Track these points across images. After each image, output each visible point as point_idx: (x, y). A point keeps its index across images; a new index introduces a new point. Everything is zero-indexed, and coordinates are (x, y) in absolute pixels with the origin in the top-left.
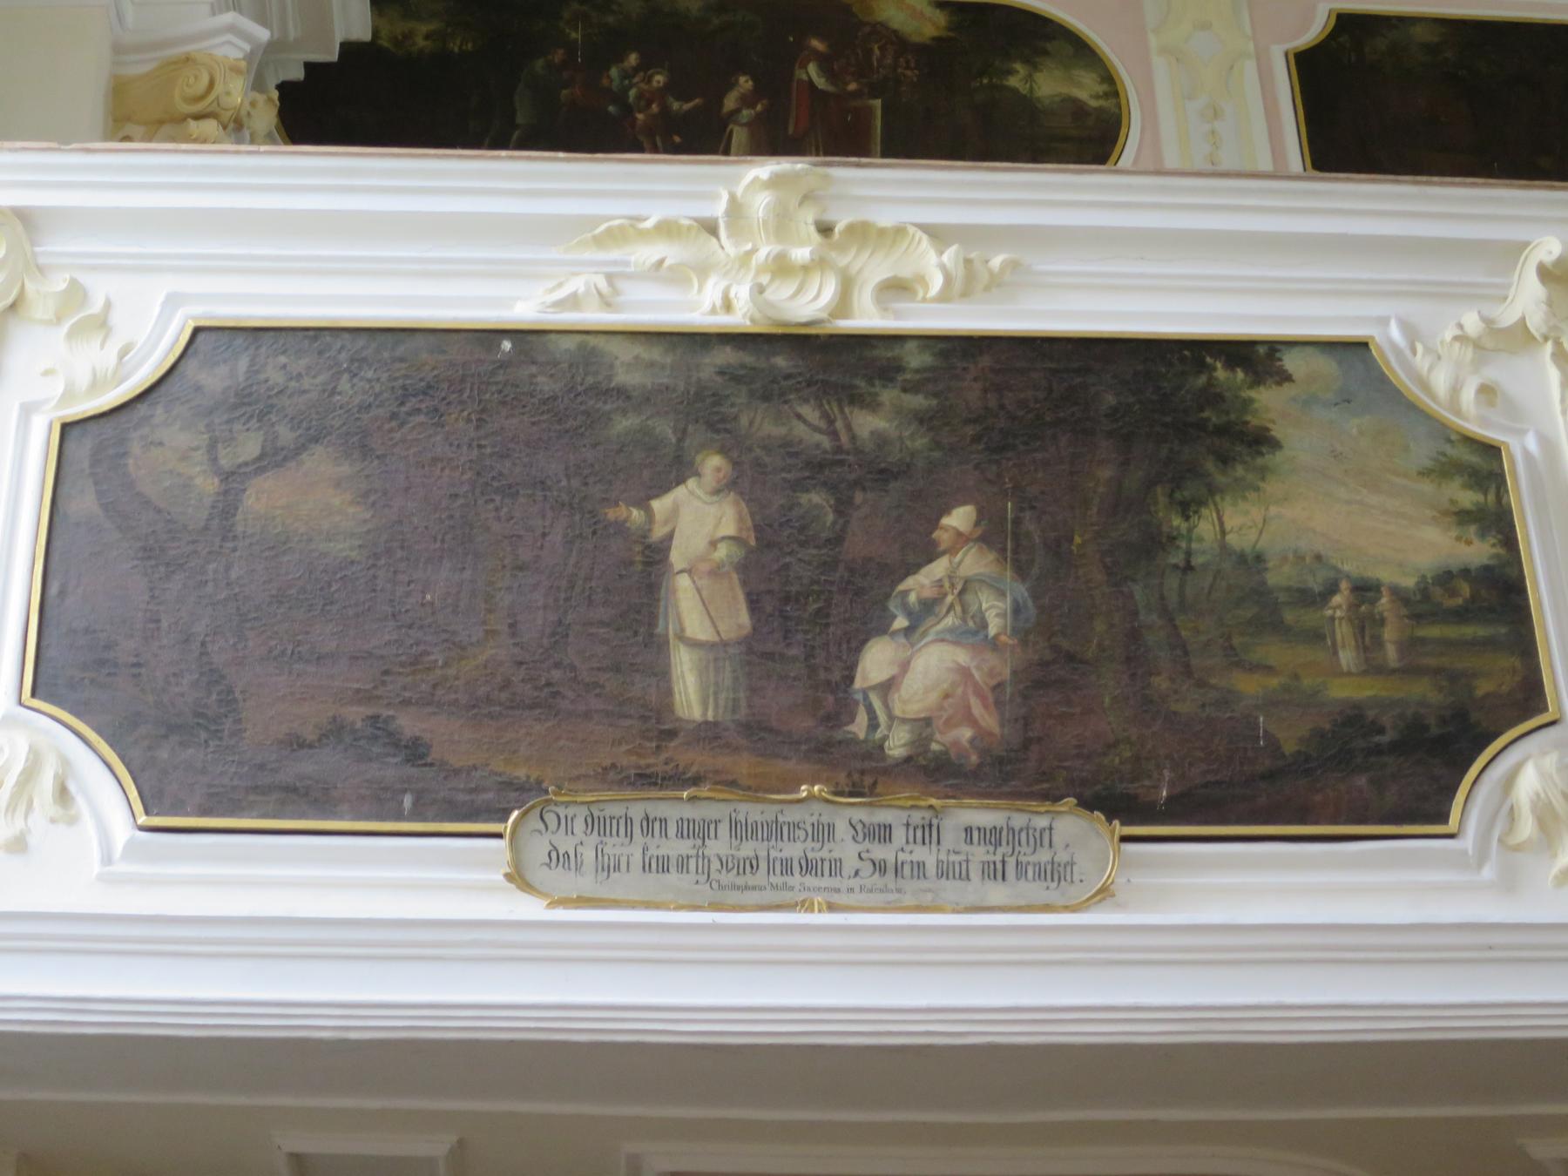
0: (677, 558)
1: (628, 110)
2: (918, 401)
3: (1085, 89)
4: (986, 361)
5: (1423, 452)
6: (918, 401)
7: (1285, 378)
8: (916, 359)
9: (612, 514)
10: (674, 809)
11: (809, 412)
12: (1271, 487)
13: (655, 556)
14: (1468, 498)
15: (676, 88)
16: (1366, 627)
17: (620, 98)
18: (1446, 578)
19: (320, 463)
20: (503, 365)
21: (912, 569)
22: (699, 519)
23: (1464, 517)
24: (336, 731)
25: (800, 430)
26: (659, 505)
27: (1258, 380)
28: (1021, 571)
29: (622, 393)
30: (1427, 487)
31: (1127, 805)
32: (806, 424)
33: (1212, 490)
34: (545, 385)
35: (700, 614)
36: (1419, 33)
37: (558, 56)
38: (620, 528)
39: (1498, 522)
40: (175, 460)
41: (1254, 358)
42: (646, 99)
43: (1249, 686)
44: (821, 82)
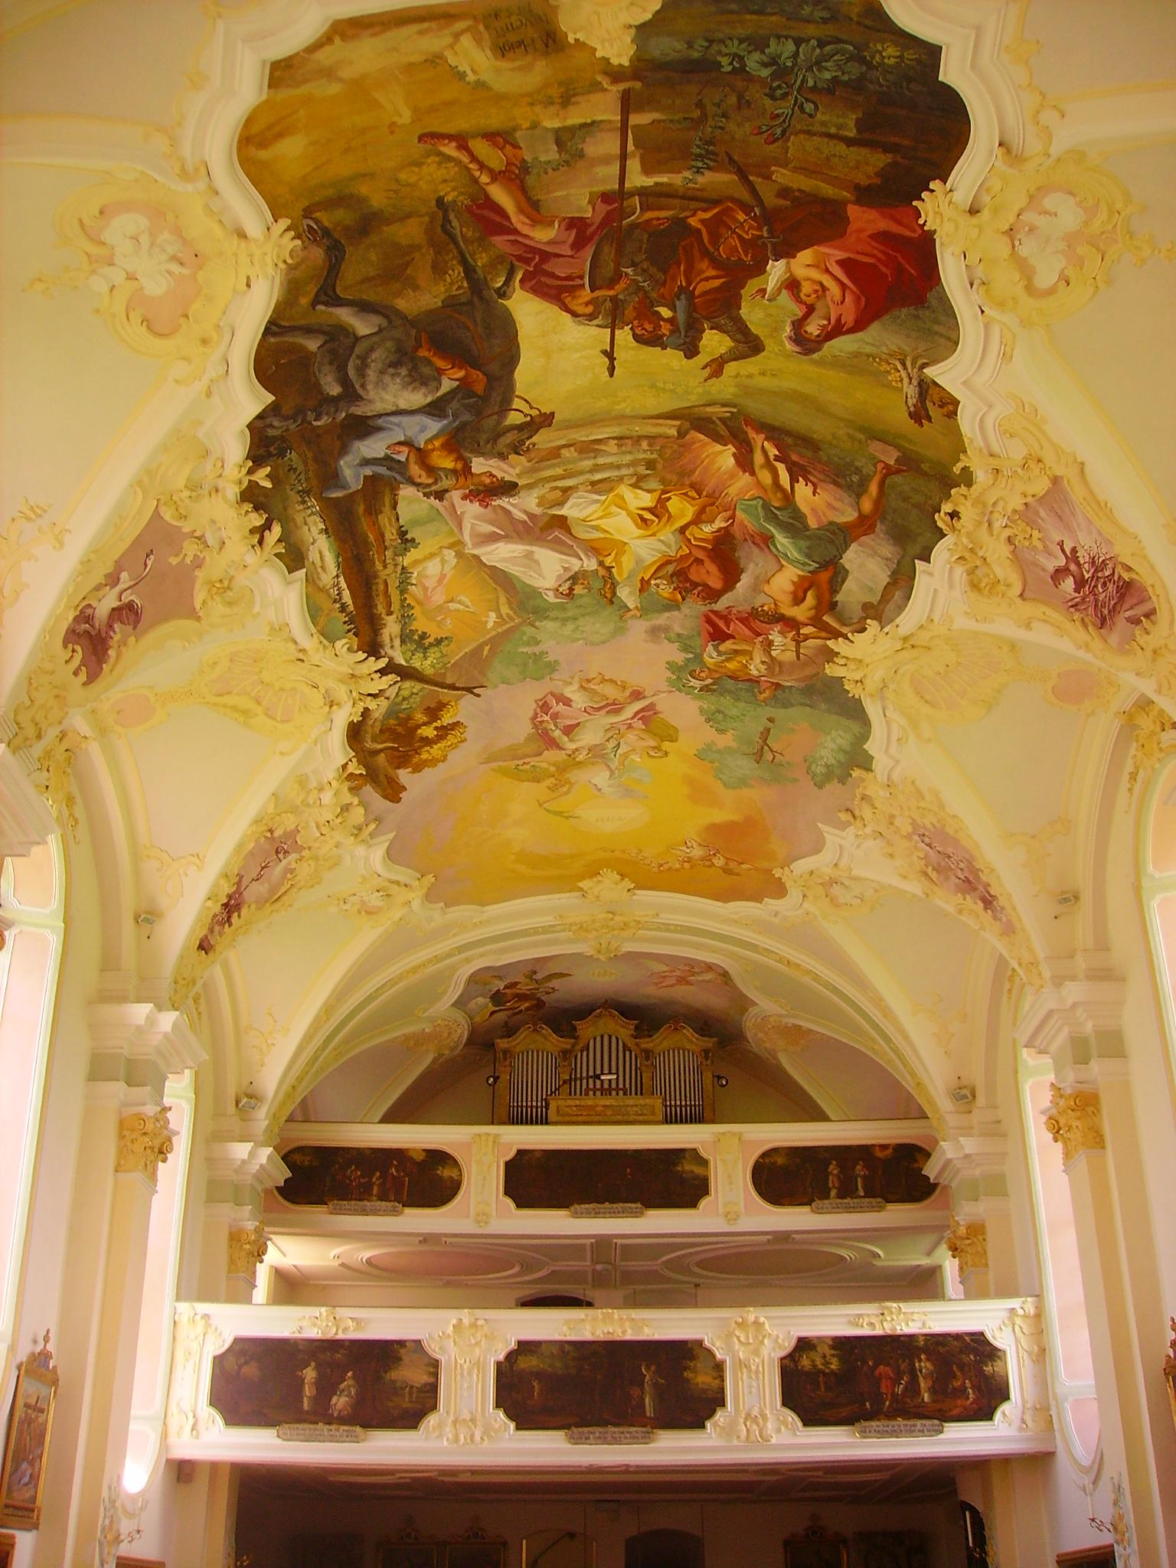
3: (454, 1174)
5: (426, 1361)
13: (303, 1380)
16: (411, 1394)
18: (426, 1385)
22: (310, 1374)
31: (367, 1426)
35: (308, 1391)
36: (538, 1155)
39: (436, 1375)
40: (231, 1363)
41: (401, 1343)
43: (391, 1404)
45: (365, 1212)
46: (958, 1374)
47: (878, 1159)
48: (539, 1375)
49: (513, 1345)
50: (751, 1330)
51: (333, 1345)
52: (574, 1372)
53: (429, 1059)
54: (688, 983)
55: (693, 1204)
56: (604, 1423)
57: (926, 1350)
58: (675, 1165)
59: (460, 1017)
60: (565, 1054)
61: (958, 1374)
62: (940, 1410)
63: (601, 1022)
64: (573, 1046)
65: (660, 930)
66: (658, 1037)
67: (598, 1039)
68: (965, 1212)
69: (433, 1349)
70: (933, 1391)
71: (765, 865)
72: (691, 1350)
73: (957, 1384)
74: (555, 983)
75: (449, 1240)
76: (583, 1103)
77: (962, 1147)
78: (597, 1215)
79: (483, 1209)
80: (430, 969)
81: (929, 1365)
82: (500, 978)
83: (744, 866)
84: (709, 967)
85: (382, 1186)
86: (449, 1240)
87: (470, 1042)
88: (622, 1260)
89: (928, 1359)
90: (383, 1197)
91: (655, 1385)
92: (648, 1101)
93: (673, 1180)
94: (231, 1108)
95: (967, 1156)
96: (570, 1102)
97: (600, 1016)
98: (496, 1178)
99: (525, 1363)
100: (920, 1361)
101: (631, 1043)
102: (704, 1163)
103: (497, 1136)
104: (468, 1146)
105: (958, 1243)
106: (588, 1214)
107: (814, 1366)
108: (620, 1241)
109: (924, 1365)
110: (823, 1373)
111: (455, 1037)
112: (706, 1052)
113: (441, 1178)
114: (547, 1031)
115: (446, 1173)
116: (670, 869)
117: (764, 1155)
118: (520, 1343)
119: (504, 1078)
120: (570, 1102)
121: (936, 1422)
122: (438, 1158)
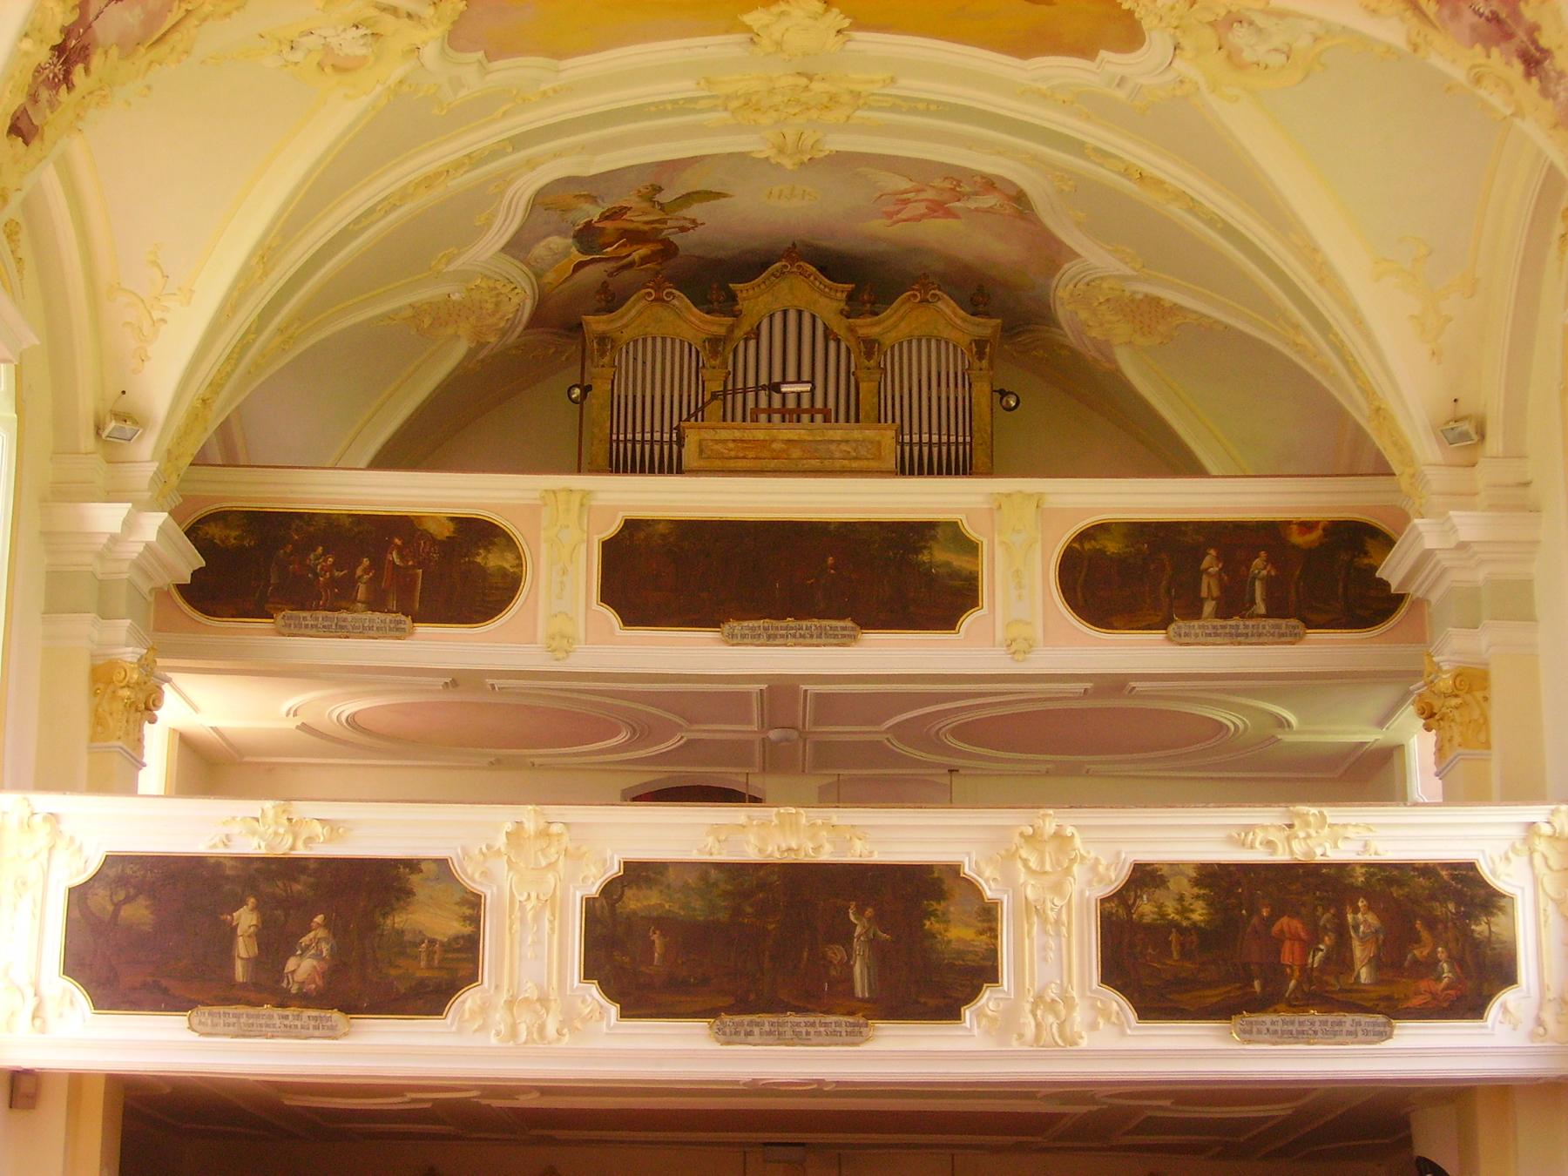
0: (239, 932)
1: (316, 575)
2: (312, 880)
3: (507, 563)
5: (457, 897)
6: (312, 880)
8: (312, 866)
10: (231, 1010)
14: (468, 912)
16: (430, 954)
18: (457, 938)
19: (142, 901)
22: (246, 919)
23: (465, 918)
24: (144, 985)
29: (227, 878)
31: (351, 1008)
32: (279, 888)
35: (244, 948)
36: (661, 528)
38: (224, 921)
39: (475, 920)
40: (101, 901)
41: (412, 865)
43: (393, 972)
44: (397, 561)
45: (343, 632)
46: (1425, 935)
47: (1294, 546)
48: (662, 922)
49: (615, 870)
50: (1049, 848)
52: (723, 916)
53: (460, 350)
54: (950, 214)
56: (776, 1006)
58: (918, 551)
60: (715, 343)
61: (1425, 935)
62: (1389, 998)
63: (784, 285)
64: (731, 329)
65: (894, 108)
66: (889, 315)
68: (1453, 648)
69: (471, 876)
70: (1377, 963)
73: (1420, 953)
74: (695, 211)
76: (747, 435)
78: (771, 639)
79: (560, 625)
81: (1372, 919)
82: (593, 199)
84: (990, 184)
87: (536, 320)
88: (816, 723)
89: (1370, 908)
90: (376, 603)
91: (873, 942)
92: (870, 434)
93: (911, 579)
94: (87, 441)
95: (1462, 546)
97: (781, 274)
98: (586, 571)
99: (637, 901)
100: (1356, 910)
101: (839, 326)
102: (972, 548)
103: (586, 494)
105: (1437, 704)
106: (755, 639)
107: (1163, 916)
108: (813, 688)
109: (1363, 919)
110: (1177, 926)
111: (508, 309)
112: (980, 345)
113: (483, 571)
114: (681, 301)
115: (493, 560)
117: (1084, 536)
118: (628, 865)
119: (601, 388)
121: (1381, 1018)
122: (477, 532)
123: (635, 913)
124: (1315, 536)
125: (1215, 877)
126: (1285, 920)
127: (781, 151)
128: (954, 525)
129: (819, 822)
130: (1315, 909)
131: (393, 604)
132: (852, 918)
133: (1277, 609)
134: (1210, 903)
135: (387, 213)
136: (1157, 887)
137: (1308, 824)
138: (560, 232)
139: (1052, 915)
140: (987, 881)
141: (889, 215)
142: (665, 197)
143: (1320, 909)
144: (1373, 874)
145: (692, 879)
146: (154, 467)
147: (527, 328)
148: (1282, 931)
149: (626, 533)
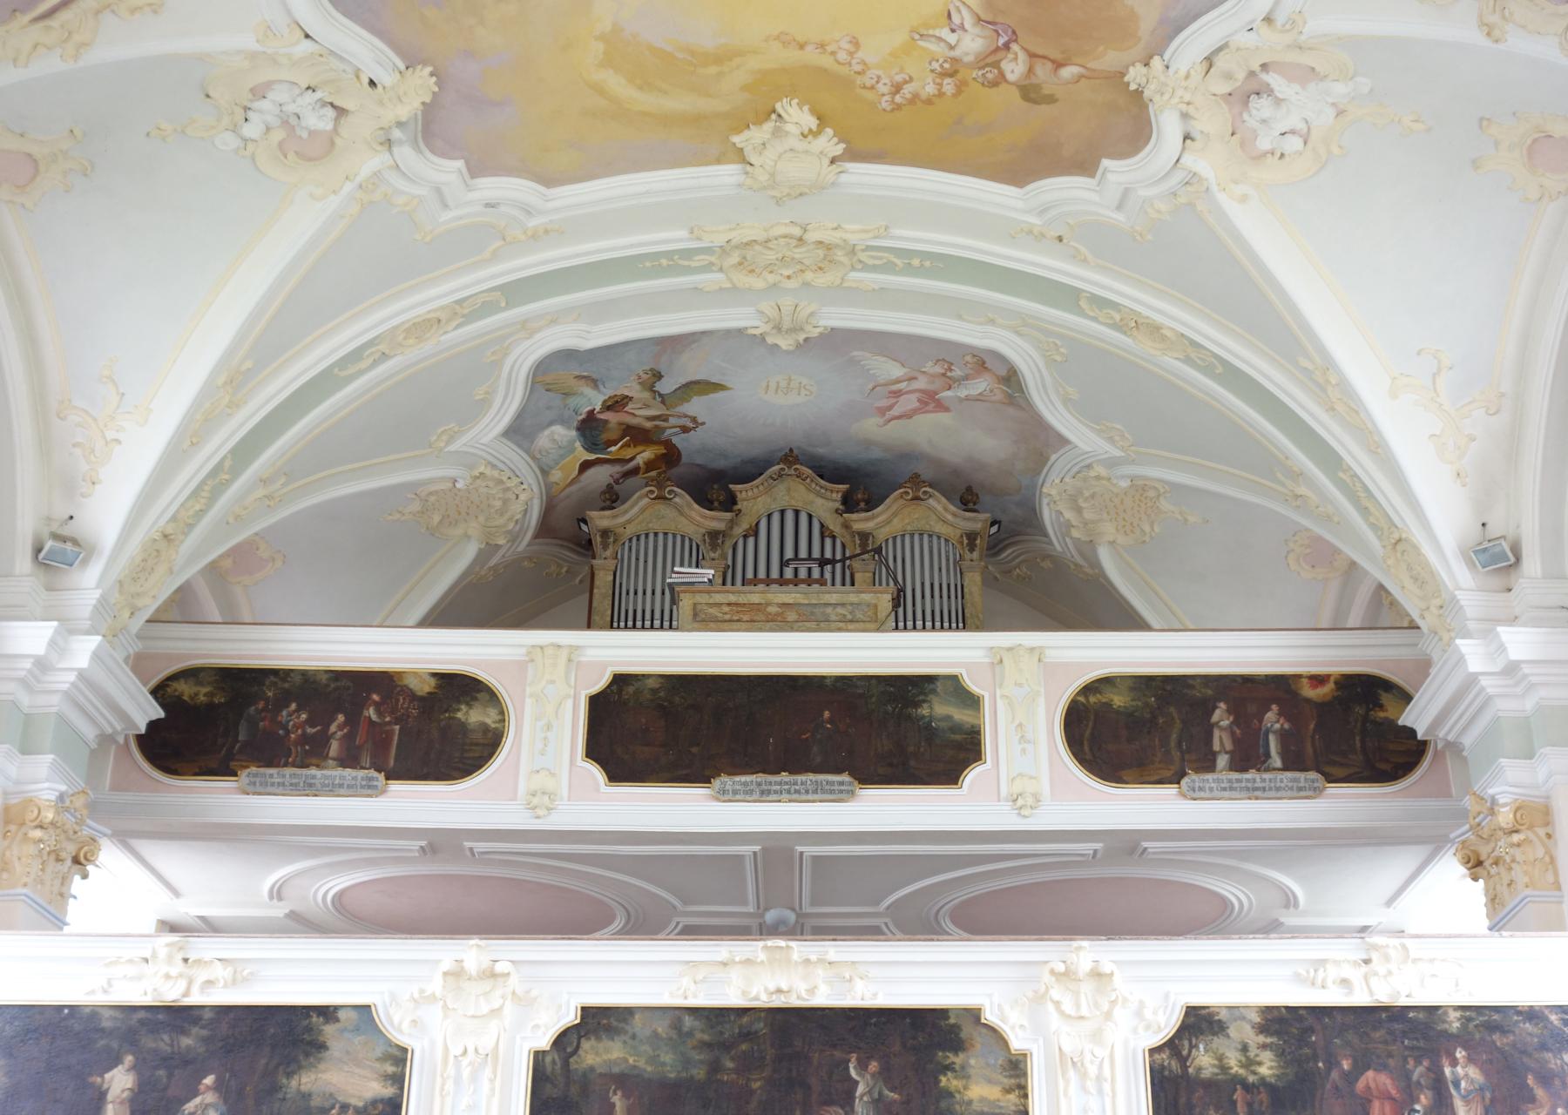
0: (110, 1097)
1: (288, 732)
2: (205, 1033)
3: (487, 717)
4: (232, 1015)
5: (379, 1052)
6: (205, 1033)
7: (338, 1020)
8: (208, 1015)
9: (91, 1079)
11: (166, 1037)
12: (322, 1066)
13: (101, 1096)
14: (390, 1069)
15: (311, 722)
17: (285, 727)
18: (374, 1102)
20: (65, 1019)
21: (188, 1100)
22: (120, 1081)
25: (162, 1045)
26: (107, 1076)
27: (327, 1021)
28: (225, 1101)
29: (103, 1030)
30: (377, 1065)
32: (164, 1043)
33: (300, 1067)
34: (77, 1027)
36: (651, 683)
37: (261, 705)
38: (93, 1084)
39: (398, 1080)
42: (296, 727)
44: (374, 717)
45: (310, 789)
46: (1540, 1093)
47: (1308, 700)
48: (624, 1080)
49: (571, 1017)
50: (1087, 988)
51: (179, 1016)
52: (699, 1073)
53: (470, 552)
54: (941, 407)
55: (950, 776)
57: (1463, 1039)
58: (917, 705)
59: (514, 456)
60: (714, 537)
63: (781, 489)
64: (732, 524)
65: (888, 268)
66: (882, 513)
67: (776, 519)
68: (1508, 783)
69: (398, 1025)
71: (1109, 59)
72: (955, 1029)
74: (695, 406)
75: (480, 846)
76: (742, 599)
77: (1502, 648)
78: (765, 795)
79: (542, 781)
80: (454, 336)
81: (1474, 1073)
82: (594, 382)
83: (1067, 72)
84: (982, 361)
85: (349, 739)
86: (480, 846)
87: (546, 529)
88: (813, 903)
89: (1470, 1060)
90: (349, 760)
92: (866, 597)
93: (908, 734)
94: (24, 563)
95: (1511, 669)
96: (718, 598)
97: (781, 475)
98: (572, 726)
99: (597, 1055)
100: (1454, 1063)
101: (834, 524)
102: (973, 702)
103: (574, 649)
104: (521, 666)
105: (1484, 851)
106: (747, 795)
107: (1224, 1068)
108: (810, 850)
109: (1464, 1073)
111: (516, 508)
112: (972, 537)
113: (463, 726)
114: (683, 498)
115: (474, 716)
116: (915, 98)
117: (1088, 689)
118: (586, 1011)
119: (603, 579)
120: (718, 598)
122: (460, 688)
123: (592, 1069)
124: (1326, 690)
125: (1286, 1024)
126: (1370, 1074)
127: (778, 328)
128: (954, 679)
129: (813, 958)
130: (1405, 1059)
131: (366, 760)
132: (853, 1073)
133: (1293, 762)
134: (1280, 1054)
135: (376, 363)
136: (1215, 1034)
137: (1387, 958)
138: (562, 421)
139: (1092, 1070)
140: (1013, 1028)
141: (882, 411)
142: (666, 387)
143: (1411, 1062)
144: (1469, 1019)
145: (662, 1027)
146: (97, 594)
147: (537, 536)
148: (1368, 1087)
149: (614, 688)
